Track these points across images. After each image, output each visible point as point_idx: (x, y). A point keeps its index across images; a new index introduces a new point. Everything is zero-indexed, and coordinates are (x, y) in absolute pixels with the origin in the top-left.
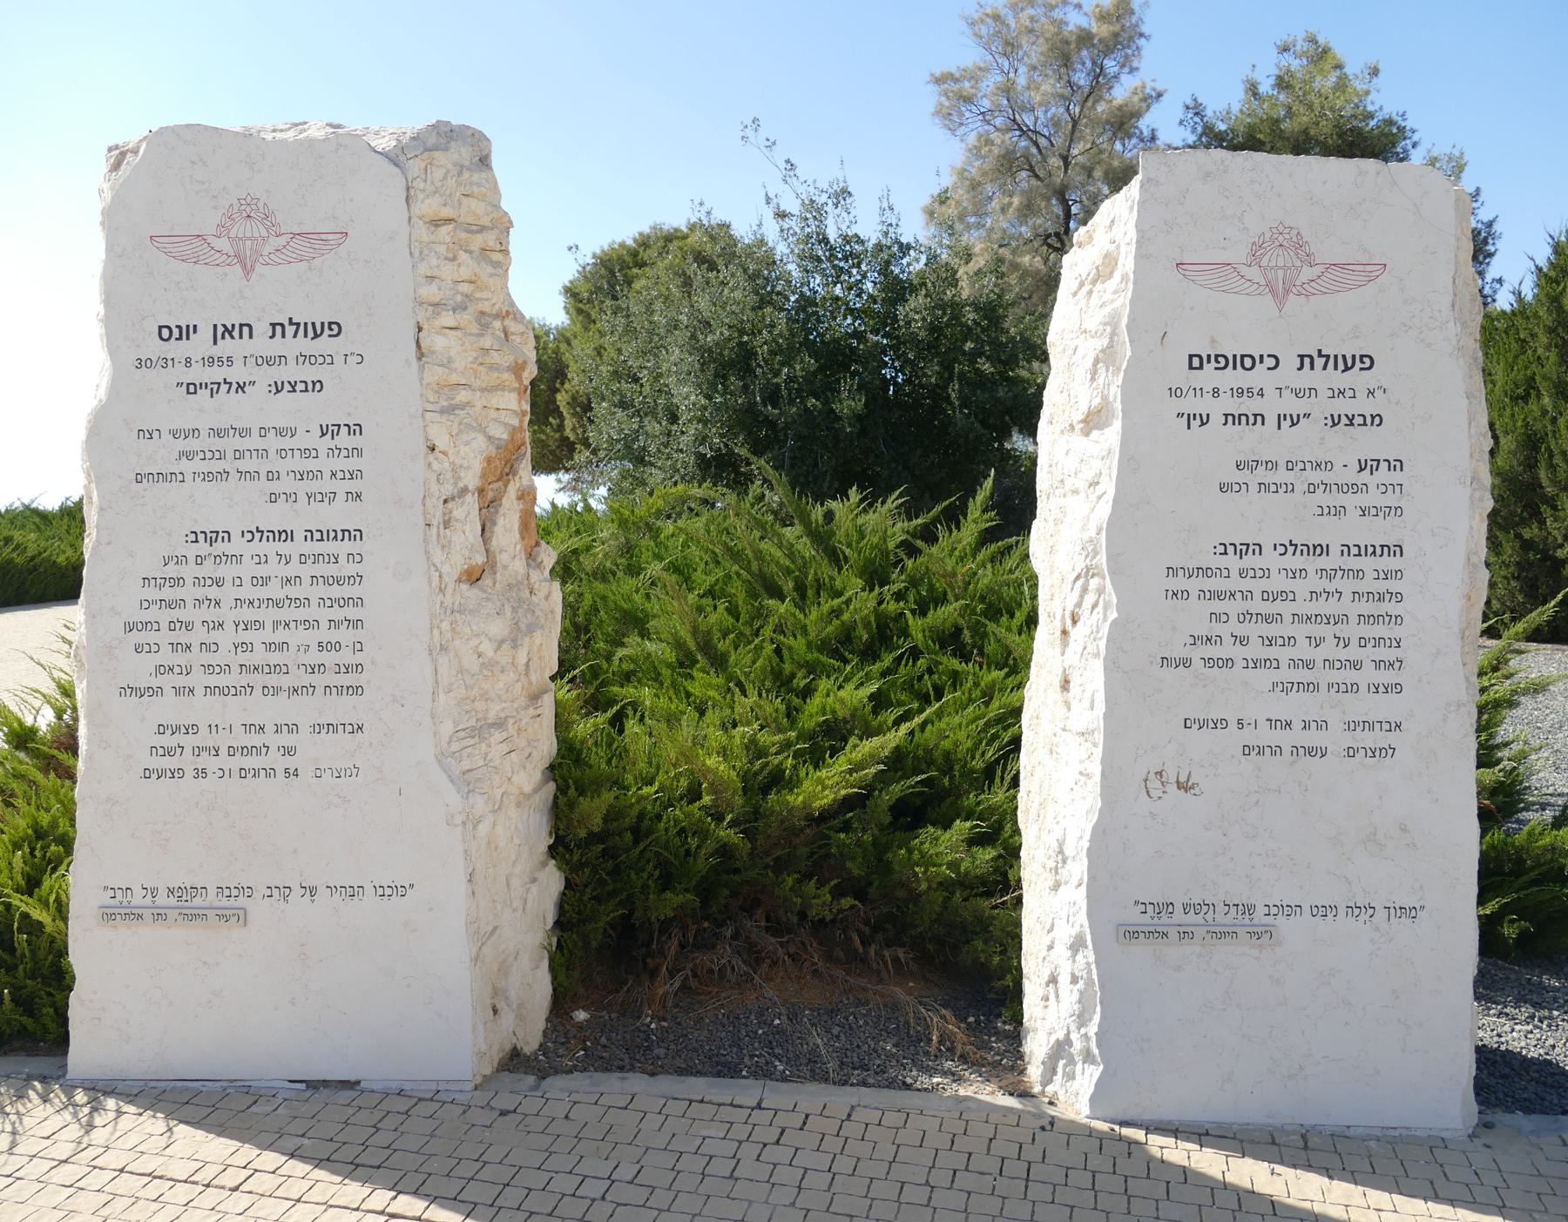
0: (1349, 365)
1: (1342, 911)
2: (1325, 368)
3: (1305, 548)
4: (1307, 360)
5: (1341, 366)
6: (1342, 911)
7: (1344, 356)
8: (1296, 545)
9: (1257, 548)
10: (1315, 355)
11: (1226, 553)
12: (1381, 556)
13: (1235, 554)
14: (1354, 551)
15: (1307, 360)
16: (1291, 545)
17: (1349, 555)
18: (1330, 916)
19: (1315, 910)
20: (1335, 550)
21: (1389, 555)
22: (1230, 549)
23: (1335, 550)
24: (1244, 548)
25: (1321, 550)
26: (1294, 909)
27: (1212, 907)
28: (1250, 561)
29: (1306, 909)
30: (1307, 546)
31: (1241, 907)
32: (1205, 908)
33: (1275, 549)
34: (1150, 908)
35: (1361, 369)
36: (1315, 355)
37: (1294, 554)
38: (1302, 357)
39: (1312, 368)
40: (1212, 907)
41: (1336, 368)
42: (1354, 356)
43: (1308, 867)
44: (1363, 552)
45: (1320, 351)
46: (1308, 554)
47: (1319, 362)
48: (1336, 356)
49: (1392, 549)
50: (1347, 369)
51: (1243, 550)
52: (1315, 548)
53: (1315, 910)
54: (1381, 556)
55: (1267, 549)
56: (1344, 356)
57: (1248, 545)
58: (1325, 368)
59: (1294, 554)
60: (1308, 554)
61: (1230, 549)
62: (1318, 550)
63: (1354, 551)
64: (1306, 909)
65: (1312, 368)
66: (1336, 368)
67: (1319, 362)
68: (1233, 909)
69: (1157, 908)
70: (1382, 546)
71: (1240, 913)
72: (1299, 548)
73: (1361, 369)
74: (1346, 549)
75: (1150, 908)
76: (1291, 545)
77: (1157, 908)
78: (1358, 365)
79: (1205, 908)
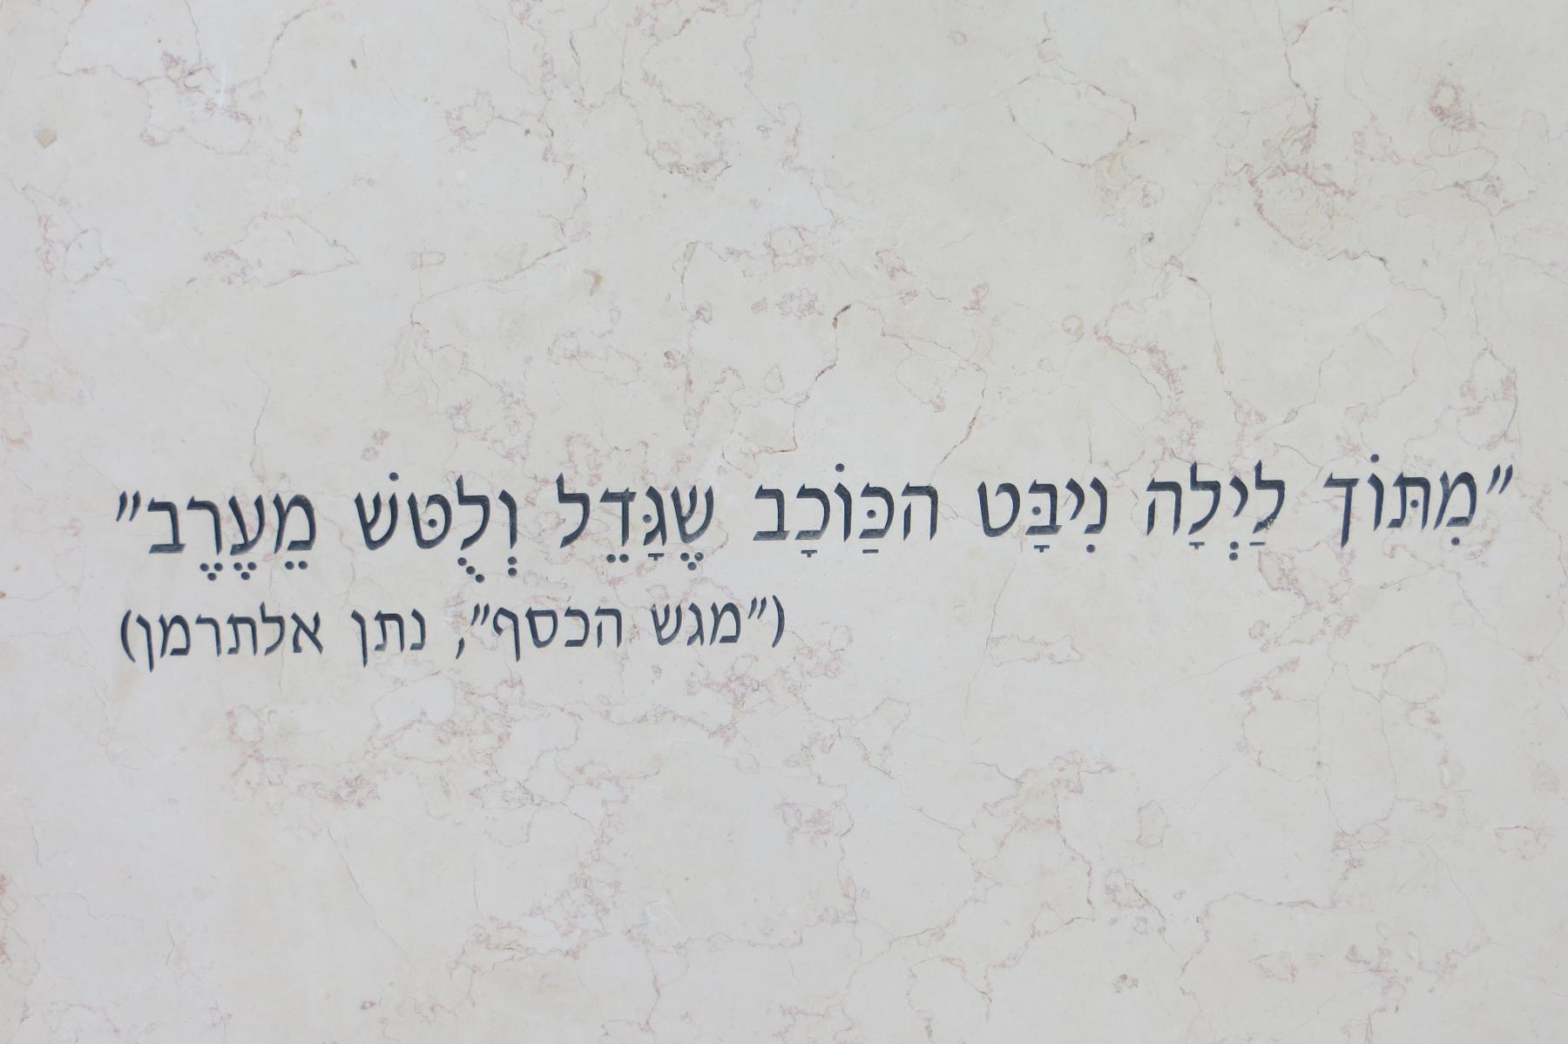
1: (1128, 505)
6: (1128, 505)
18: (1072, 530)
19: (1000, 507)
26: (900, 503)
27: (499, 511)
29: (959, 503)
31: (642, 506)
32: (466, 518)
34: (195, 526)
40: (499, 511)
43: (976, 305)
53: (1000, 507)
64: (959, 503)
68: (606, 517)
69: (231, 534)
71: (639, 529)
75: (195, 526)
77: (231, 534)
79: (466, 518)
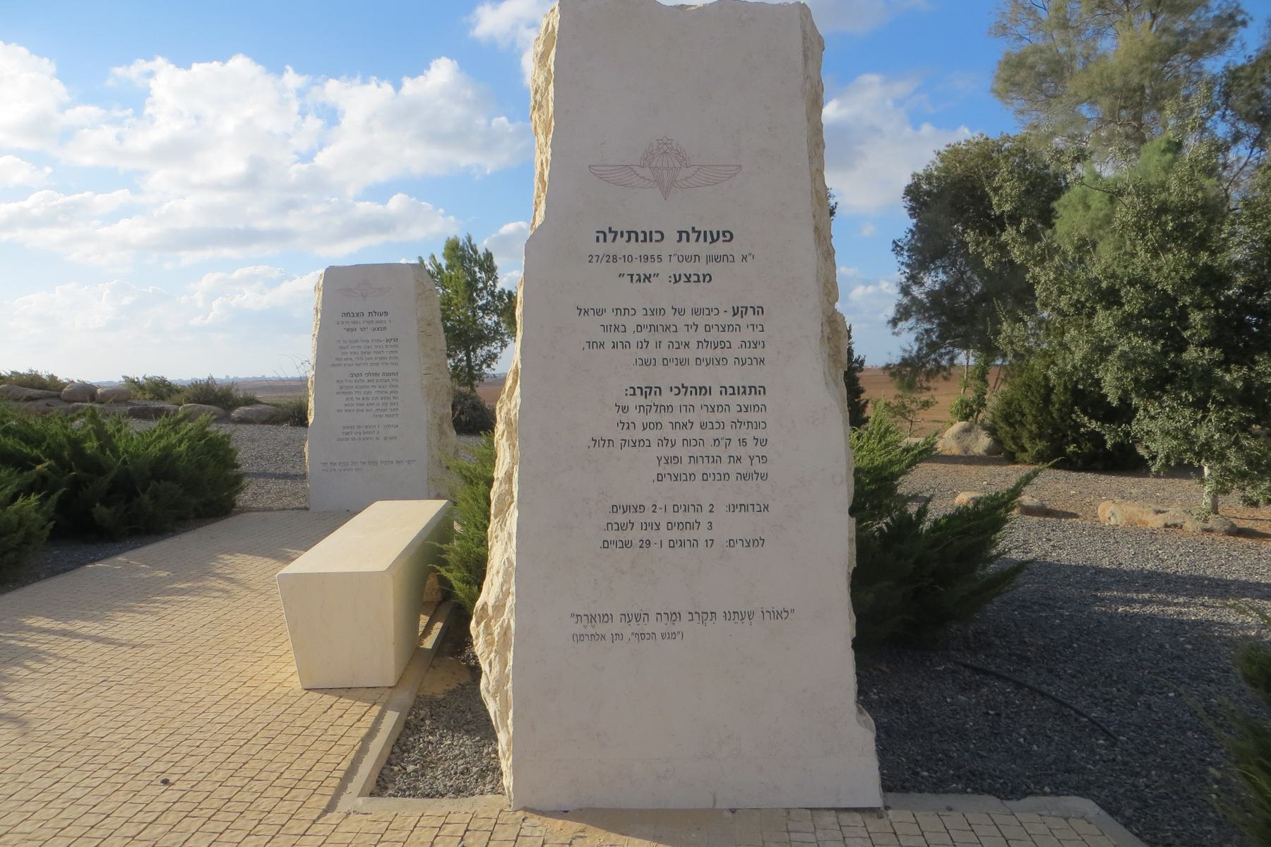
0: (715, 237)
2: (697, 240)
3: (694, 390)
4: (684, 235)
5: (709, 239)
7: (711, 232)
8: (687, 388)
9: (658, 390)
10: (690, 232)
11: (634, 394)
12: (750, 394)
13: (642, 394)
14: (730, 391)
15: (684, 235)
16: (683, 387)
17: (726, 393)
20: (716, 390)
21: (756, 393)
22: (638, 391)
23: (716, 390)
24: (648, 390)
25: (704, 390)
28: (652, 399)
30: (695, 388)
33: (671, 391)
35: (724, 241)
36: (690, 232)
37: (685, 394)
38: (680, 233)
39: (688, 240)
41: (705, 240)
42: (718, 232)
44: (736, 392)
45: (693, 228)
46: (696, 394)
47: (693, 236)
48: (705, 232)
49: (758, 389)
50: (713, 241)
51: (646, 391)
52: (701, 388)
54: (750, 394)
55: (665, 391)
56: (711, 233)
57: (651, 388)
58: (697, 240)
59: (685, 394)
60: (696, 394)
61: (638, 391)
62: (703, 391)
63: (730, 391)
65: (688, 240)
66: (705, 240)
67: (693, 236)
70: (750, 387)
72: (689, 390)
73: (724, 241)
74: (723, 390)
76: (683, 387)
78: (722, 238)
